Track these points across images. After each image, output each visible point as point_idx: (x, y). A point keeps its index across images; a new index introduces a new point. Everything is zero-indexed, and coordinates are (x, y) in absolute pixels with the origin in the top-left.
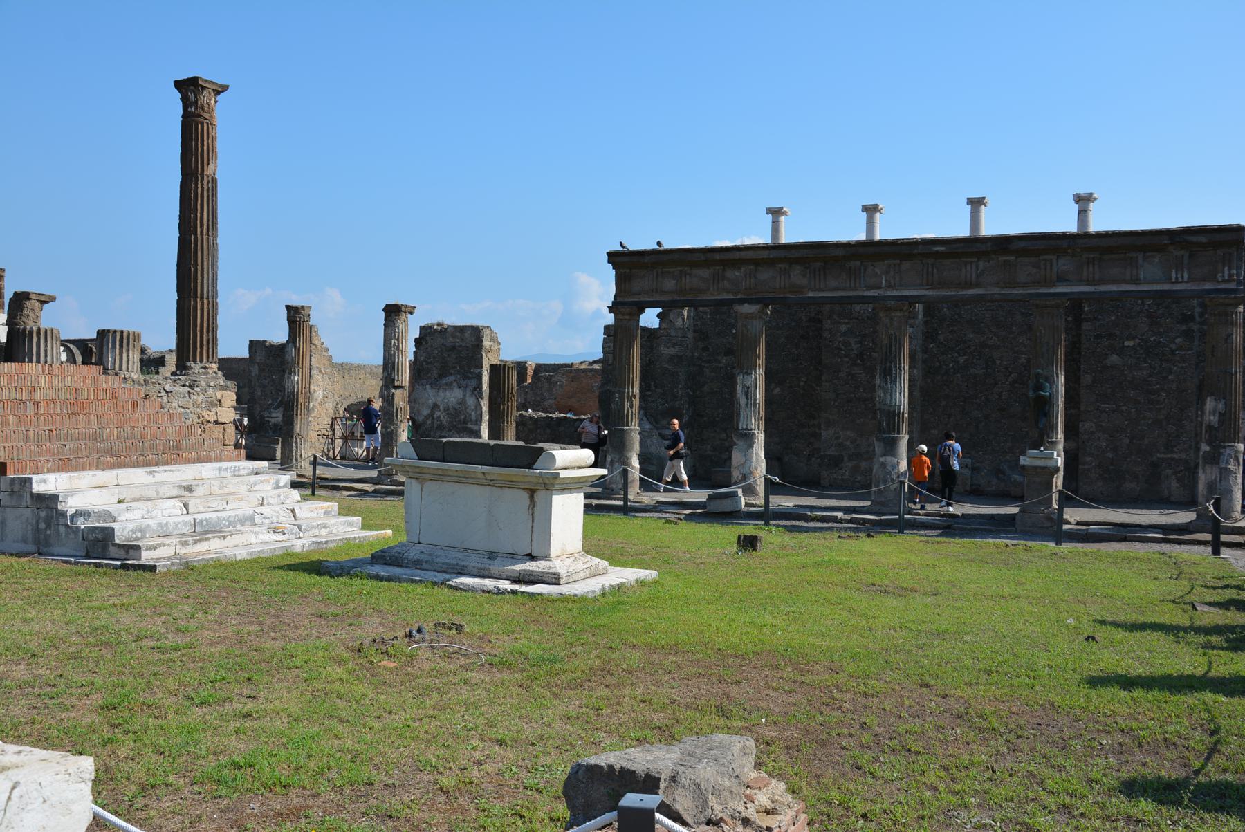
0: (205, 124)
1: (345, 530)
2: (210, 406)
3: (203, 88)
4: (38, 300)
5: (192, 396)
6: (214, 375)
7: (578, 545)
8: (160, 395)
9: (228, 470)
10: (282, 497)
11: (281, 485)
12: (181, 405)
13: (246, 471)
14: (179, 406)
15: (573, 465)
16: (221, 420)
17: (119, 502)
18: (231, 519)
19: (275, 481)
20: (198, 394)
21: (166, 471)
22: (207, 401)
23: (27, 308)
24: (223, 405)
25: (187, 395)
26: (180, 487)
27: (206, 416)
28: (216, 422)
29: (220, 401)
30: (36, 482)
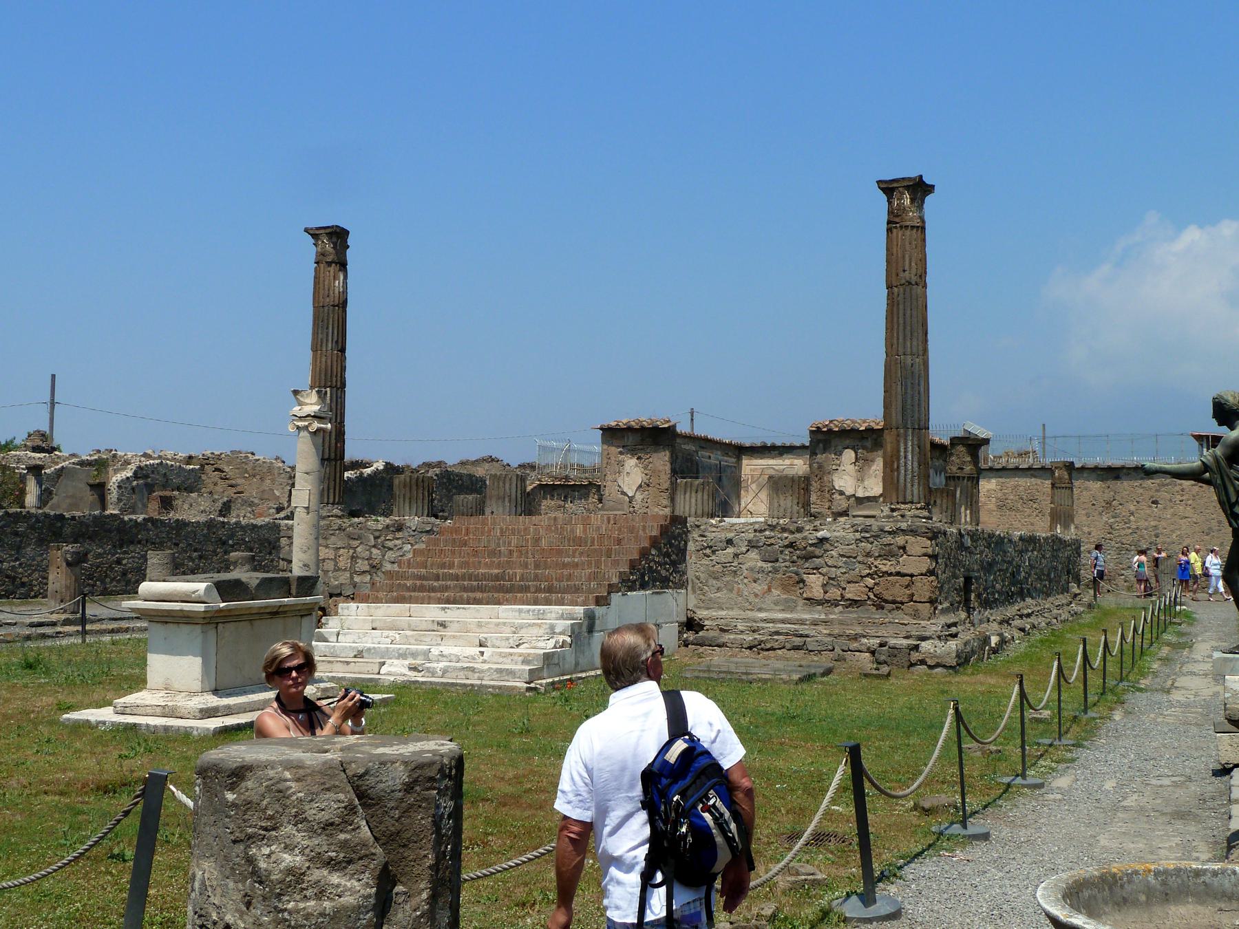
1: (502, 679)
2: (888, 554)
7: (197, 686)
8: (810, 542)
10: (511, 641)
11: (557, 630)
13: (554, 615)
15: (165, 599)
16: (902, 571)
17: (373, 629)
18: (401, 652)
19: (547, 626)
21: (459, 608)
22: (883, 549)
24: (909, 553)
26: (433, 621)
27: (880, 566)
28: (898, 574)
29: (904, 548)
30: (342, 608)
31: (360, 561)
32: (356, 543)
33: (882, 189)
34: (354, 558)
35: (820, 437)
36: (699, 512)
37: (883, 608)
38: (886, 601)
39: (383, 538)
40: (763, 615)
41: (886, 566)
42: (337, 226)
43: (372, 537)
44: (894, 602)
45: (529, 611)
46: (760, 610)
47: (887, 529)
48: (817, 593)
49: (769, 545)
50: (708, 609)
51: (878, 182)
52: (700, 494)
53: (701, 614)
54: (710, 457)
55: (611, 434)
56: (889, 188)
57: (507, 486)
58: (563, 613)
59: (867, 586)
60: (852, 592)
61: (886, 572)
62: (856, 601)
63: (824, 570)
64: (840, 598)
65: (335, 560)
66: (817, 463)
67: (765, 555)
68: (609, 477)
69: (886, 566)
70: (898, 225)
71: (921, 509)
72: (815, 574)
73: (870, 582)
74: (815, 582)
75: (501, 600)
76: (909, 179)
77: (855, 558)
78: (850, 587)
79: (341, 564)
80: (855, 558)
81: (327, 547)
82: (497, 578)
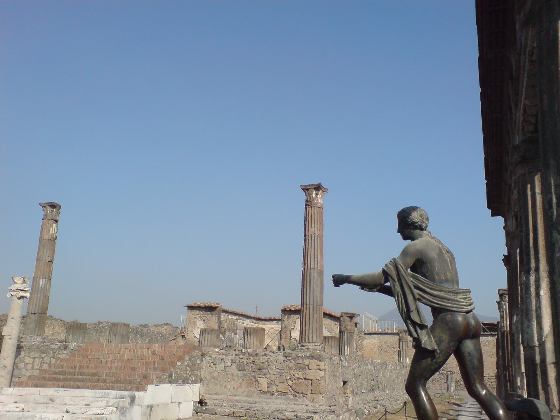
0: (308, 208)
3: (307, 190)
4: (347, 316)
5: (286, 363)
6: (306, 350)
8: (262, 361)
9: (101, 394)
10: (82, 410)
11: (110, 404)
12: (277, 367)
14: (276, 368)
16: (307, 377)
20: (290, 362)
23: (342, 321)
24: (310, 368)
25: (283, 362)
29: (308, 365)
31: (45, 365)
32: (44, 355)
33: (303, 189)
34: (42, 363)
35: (286, 312)
36: (209, 345)
37: (296, 396)
38: (298, 393)
39: (57, 353)
40: (237, 398)
41: (299, 374)
42: (53, 202)
43: (52, 352)
44: (303, 394)
45: (100, 393)
46: (235, 396)
47: (300, 355)
48: (265, 388)
49: (241, 362)
50: (210, 394)
51: (301, 186)
52: (210, 336)
53: (206, 398)
54: (244, 323)
55: (191, 308)
56: (306, 189)
57: (119, 329)
58: (116, 395)
59: (289, 385)
60: (282, 387)
61: (299, 378)
62: (283, 392)
63: (268, 376)
64: (275, 391)
65: (33, 364)
66: (285, 325)
67: (239, 367)
68: (189, 329)
69: (299, 374)
70: (310, 206)
71: (317, 345)
72: (263, 378)
73: (290, 383)
74: (264, 382)
75: (90, 387)
76: (315, 185)
77: (283, 370)
78: (280, 385)
79: (35, 367)
80: (283, 370)
81: (29, 357)
82: (94, 374)
